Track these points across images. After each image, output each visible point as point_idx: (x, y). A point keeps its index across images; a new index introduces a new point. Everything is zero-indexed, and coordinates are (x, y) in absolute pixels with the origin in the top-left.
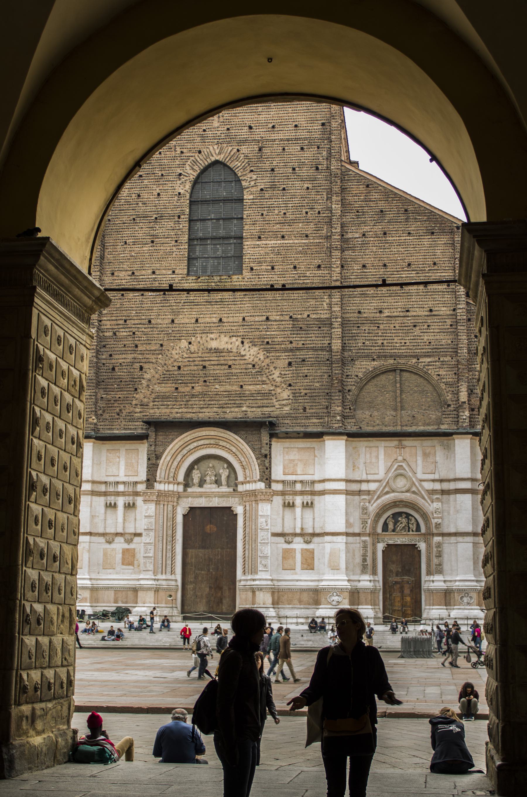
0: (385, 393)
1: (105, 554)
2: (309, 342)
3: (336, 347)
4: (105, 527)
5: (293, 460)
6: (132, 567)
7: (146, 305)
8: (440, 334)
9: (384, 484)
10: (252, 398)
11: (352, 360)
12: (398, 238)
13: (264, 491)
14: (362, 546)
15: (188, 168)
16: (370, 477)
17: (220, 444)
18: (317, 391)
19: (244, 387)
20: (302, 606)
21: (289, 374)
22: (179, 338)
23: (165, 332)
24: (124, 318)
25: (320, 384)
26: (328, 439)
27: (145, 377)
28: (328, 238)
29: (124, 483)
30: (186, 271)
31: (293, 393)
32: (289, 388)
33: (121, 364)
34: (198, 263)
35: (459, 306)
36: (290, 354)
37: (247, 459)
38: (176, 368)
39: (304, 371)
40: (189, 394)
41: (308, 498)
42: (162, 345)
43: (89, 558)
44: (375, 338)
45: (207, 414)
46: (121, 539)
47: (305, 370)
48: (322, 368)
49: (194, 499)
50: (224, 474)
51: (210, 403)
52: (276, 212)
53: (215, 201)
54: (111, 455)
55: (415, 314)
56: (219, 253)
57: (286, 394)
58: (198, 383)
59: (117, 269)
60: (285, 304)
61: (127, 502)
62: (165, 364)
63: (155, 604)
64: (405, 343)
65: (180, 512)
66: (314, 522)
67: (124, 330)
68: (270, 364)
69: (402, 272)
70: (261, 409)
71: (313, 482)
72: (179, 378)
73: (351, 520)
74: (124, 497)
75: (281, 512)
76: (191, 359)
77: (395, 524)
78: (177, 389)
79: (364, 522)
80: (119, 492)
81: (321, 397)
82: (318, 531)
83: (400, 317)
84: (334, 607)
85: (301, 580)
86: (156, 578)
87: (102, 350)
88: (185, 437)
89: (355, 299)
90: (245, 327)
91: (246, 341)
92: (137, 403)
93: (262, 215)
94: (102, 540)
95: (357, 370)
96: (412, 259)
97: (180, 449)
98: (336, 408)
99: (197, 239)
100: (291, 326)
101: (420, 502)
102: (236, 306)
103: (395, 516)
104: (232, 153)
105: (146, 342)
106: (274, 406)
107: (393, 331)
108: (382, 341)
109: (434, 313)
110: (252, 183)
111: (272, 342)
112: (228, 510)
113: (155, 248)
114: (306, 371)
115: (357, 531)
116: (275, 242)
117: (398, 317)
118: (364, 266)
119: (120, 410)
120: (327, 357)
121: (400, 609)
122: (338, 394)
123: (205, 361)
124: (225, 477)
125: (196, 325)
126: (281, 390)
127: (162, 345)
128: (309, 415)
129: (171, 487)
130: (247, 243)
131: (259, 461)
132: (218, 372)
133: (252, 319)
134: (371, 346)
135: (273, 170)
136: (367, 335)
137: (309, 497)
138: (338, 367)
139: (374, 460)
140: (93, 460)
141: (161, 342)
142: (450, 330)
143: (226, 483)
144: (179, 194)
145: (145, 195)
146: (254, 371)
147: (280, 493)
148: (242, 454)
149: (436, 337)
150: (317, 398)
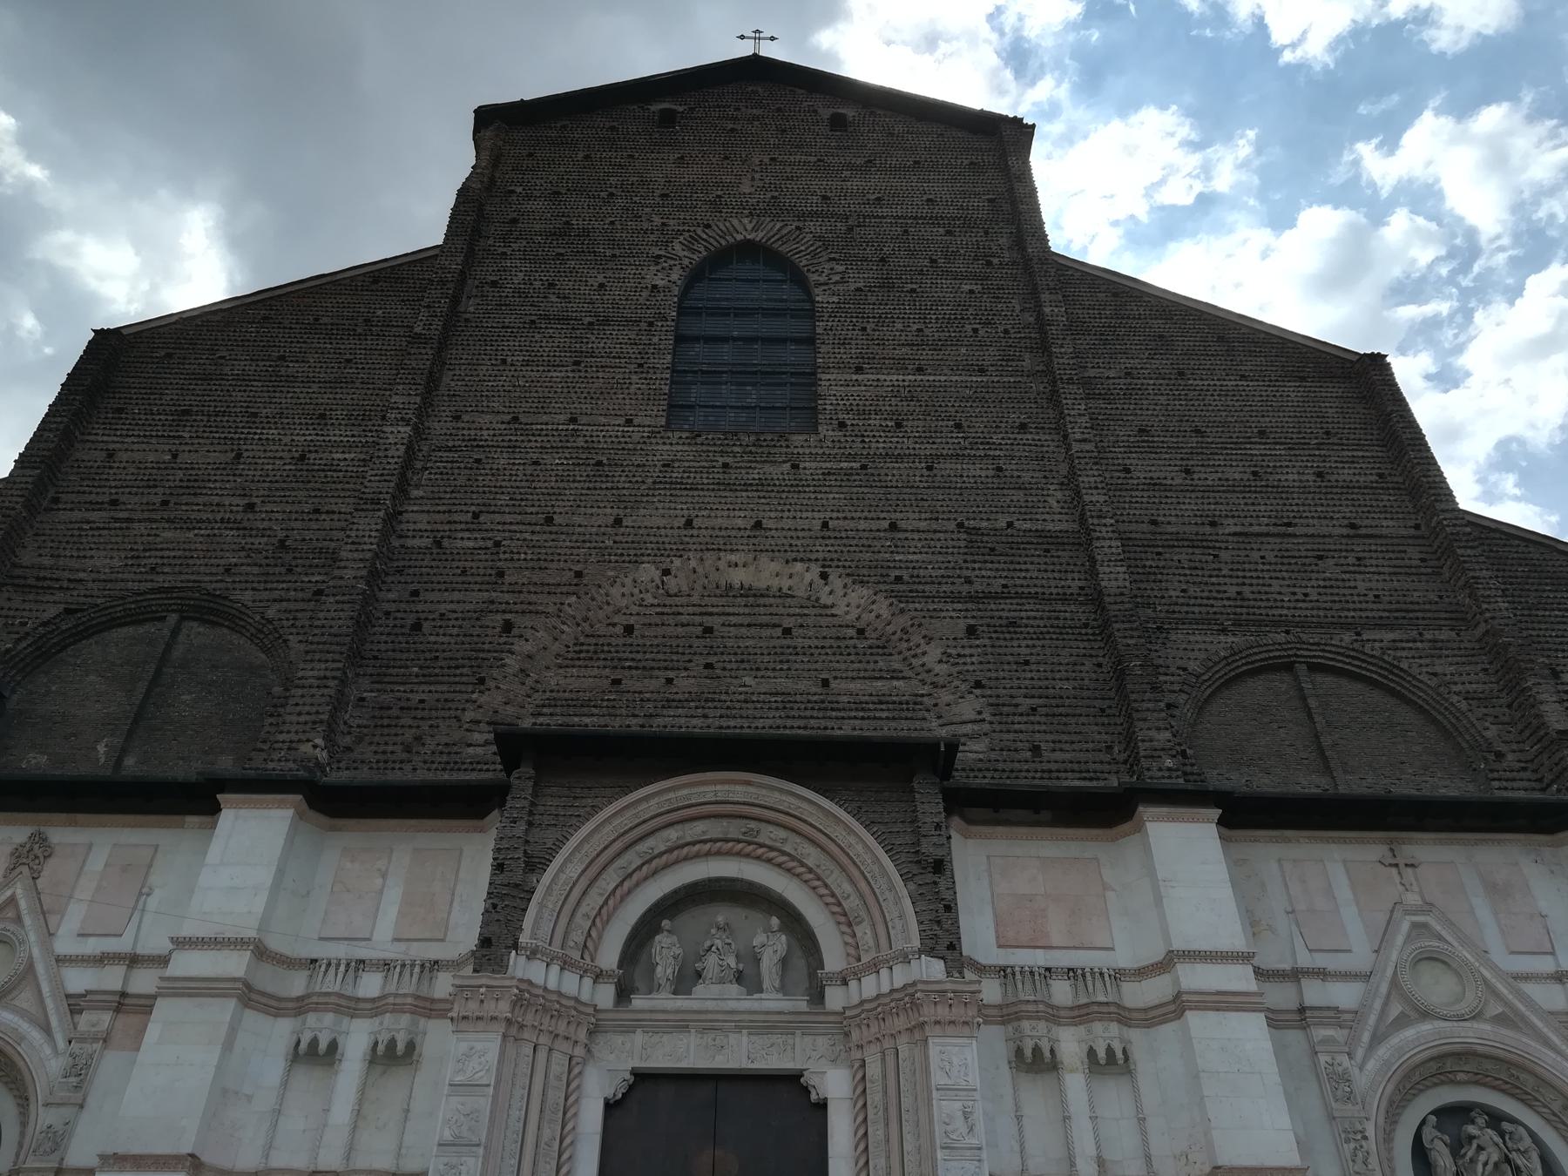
0: (1275, 726)
3: (1114, 583)
4: (269, 1147)
7: (540, 484)
8: (1400, 578)
9: (1384, 988)
10: (861, 714)
11: (1158, 628)
13: (949, 986)
15: (678, 247)
16: (1321, 961)
17: (760, 840)
18: (1067, 702)
19: (833, 684)
21: (971, 655)
23: (594, 544)
24: (473, 508)
26: (1158, 819)
27: (516, 648)
29: (386, 966)
30: (663, 421)
31: (992, 705)
32: (978, 692)
36: (969, 606)
37: (863, 885)
38: (619, 630)
39: (1016, 650)
40: (655, 696)
41: (1106, 1034)
42: (579, 574)
44: (1214, 580)
48: (1073, 644)
49: (656, 1038)
50: (773, 946)
55: (1311, 531)
57: (968, 708)
58: (686, 669)
60: (941, 497)
61: (384, 1038)
64: (1306, 595)
65: (597, 1089)
66: (1144, 1133)
67: (466, 535)
68: (910, 630)
71: (1118, 975)
74: (377, 1020)
78: (617, 682)
80: (358, 1000)
81: (1083, 720)
83: (1273, 535)
89: (1134, 494)
93: (864, 329)
97: (618, 845)
98: (1153, 733)
100: (962, 544)
101: (1547, 1060)
102: (802, 495)
105: (531, 564)
109: (1363, 531)
111: (912, 576)
112: (792, 1081)
113: (582, 374)
114: (1024, 651)
116: (901, 377)
117: (1267, 535)
119: (418, 739)
123: (711, 614)
124: (776, 959)
126: (952, 697)
128: (1053, 766)
129: (570, 983)
131: (912, 886)
132: (750, 642)
134: (1208, 598)
136: (1188, 572)
138: (1132, 629)
140: (280, 873)
141: (578, 568)
142: (1423, 570)
143: (777, 984)
144: (655, 287)
146: (861, 644)
147: (994, 1012)
148: (843, 869)
150: (1073, 720)
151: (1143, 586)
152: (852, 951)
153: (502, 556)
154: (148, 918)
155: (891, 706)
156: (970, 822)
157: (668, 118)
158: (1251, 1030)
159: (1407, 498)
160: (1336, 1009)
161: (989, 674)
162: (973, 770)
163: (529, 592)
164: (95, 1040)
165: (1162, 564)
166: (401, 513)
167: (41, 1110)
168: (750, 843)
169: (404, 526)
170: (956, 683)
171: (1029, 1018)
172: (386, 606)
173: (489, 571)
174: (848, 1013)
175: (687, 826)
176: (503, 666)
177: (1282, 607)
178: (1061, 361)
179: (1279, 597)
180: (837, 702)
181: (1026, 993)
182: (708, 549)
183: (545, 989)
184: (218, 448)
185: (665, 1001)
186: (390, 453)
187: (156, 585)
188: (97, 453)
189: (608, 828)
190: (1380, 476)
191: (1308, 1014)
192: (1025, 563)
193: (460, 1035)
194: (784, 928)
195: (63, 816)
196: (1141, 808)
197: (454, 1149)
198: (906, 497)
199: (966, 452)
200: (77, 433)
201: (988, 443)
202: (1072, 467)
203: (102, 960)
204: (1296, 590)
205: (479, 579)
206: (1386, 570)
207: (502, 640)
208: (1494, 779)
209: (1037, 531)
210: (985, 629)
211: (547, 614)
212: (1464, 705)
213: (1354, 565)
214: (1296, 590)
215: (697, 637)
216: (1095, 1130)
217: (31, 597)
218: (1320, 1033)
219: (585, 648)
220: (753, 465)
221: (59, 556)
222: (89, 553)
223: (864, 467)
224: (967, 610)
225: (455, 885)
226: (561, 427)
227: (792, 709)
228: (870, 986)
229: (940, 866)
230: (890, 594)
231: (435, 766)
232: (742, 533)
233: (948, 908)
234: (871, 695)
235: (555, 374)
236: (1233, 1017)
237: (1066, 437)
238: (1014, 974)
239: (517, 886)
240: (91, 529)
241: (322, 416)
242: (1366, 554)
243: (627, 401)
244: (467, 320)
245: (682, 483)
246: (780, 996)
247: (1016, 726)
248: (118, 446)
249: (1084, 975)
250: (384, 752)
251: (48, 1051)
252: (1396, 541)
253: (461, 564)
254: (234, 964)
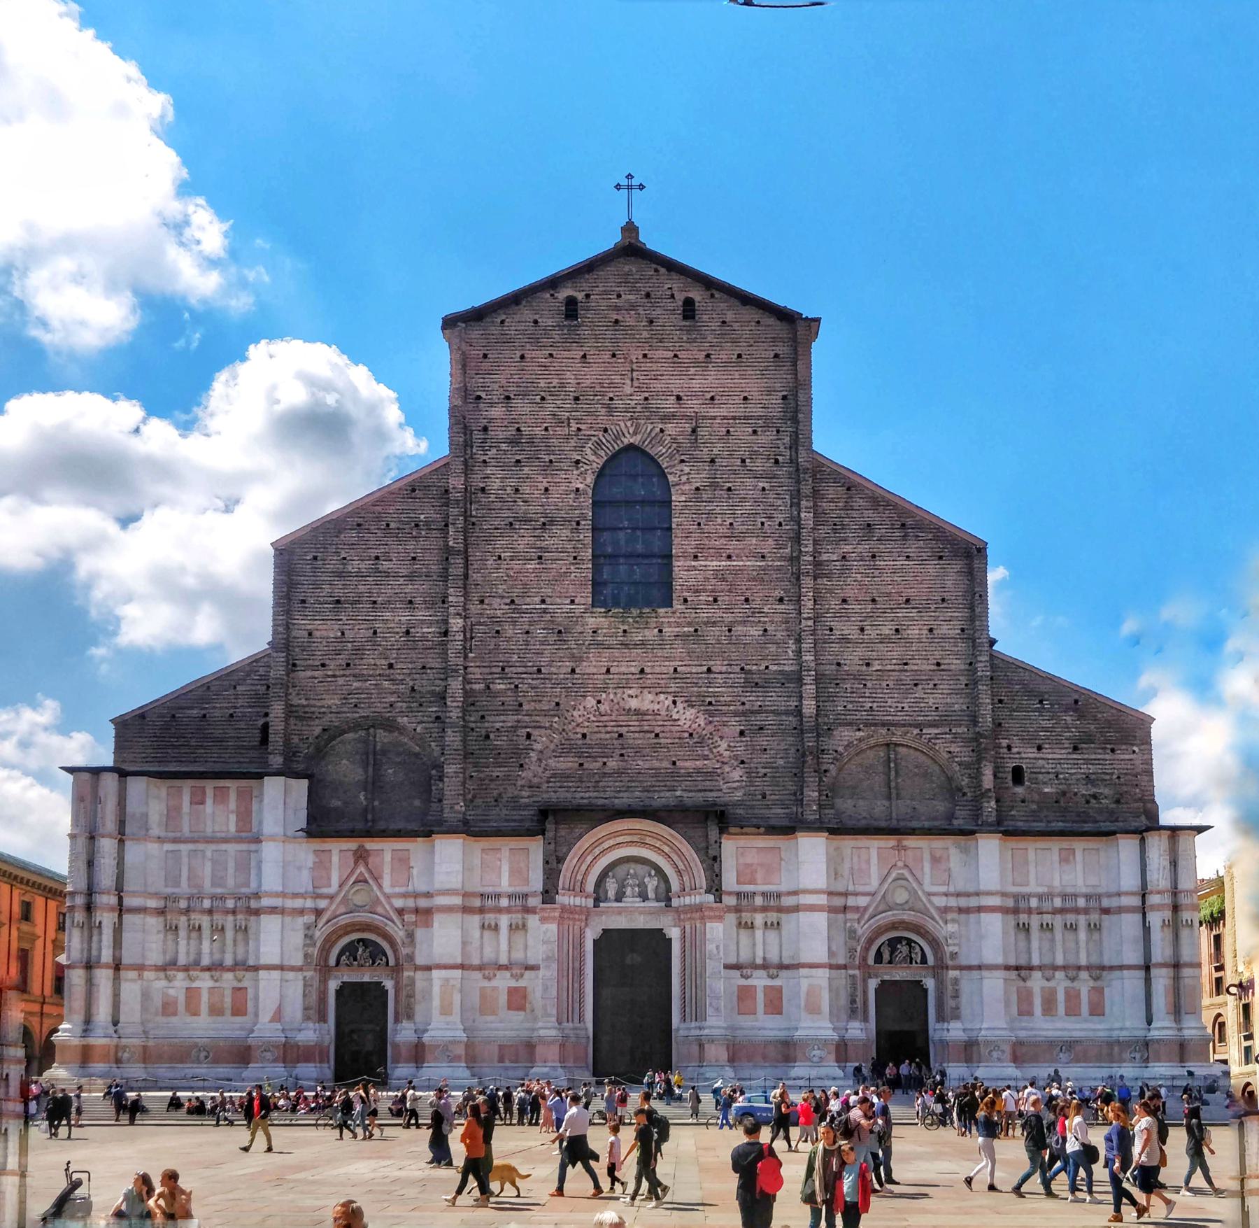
1: (483, 996)
5: (752, 865)
6: (522, 1013)
11: (829, 729)
12: (892, 563)
15: (589, 451)
16: (860, 889)
19: (678, 763)
20: (767, 1064)
27: (534, 747)
28: (794, 560)
34: (607, 591)
35: (980, 658)
36: (743, 718)
38: (579, 736)
41: (773, 917)
42: (558, 704)
45: (624, 800)
46: (507, 974)
47: (763, 741)
50: (652, 884)
51: (629, 784)
52: (719, 521)
53: (629, 503)
55: (915, 668)
56: (637, 577)
57: (737, 774)
62: (564, 730)
70: (702, 794)
71: (779, 895)
73: (834, 948)
76: (600, 724)
78: (581, 765)
79: (852, 951)
82: (786, 961)
85: (765, 1029)
87: (469, 709)
91: (679, 700)
93: (699, 524)
94: (477, 975)
96: (911, 593)
98: (811, 793)
99: (605, 557)
100: (742, 681)
101: (930, 925)
103: (893, 943)
104: (653, 434)
106: (721, 790)
108: (870, 705)
109: (942, 667)
110: (684, 478)
114: (766, 743)
115: (841, 961)
116: (718, 563)
118: (844, 601)
119: (500, 795)
122: (813, 774)
125: (606, 676)
127: (558, 704)
129: (578, 901)
130: (678, 564)
132: (640, 742)
133: (688, 669)
135: (713, 461)
137: (775, 914)
139: (864, 866)
141: (557, 700)
144: (578, 490)
145: (525, 489)
148: (679, 856)
157: (571, 303)
158: (821, 919)
178: (805, 558)
186: (457, 638)
190: (963, 630)
204: (899, 705)
211: (546, 728)
212: (957, 768)
216: (764, 950)
222: (324, 696)
223: (696, 631)
228: (687, 900)
229: (715, 859)
232: (634, 677)
235: (529, 566)
236: (816, 914)
237: (800, 613)
241: (411, 602)
244: (474, 524)
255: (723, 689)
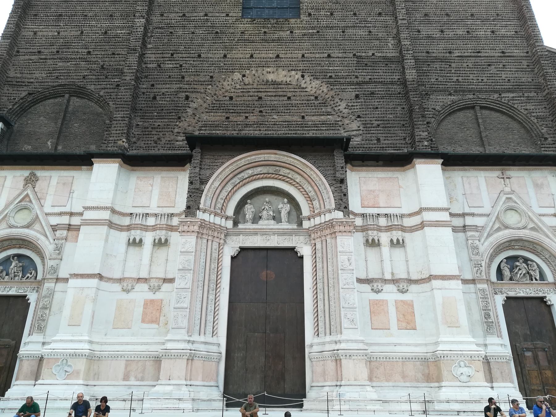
0: (466, 129)
2: (378, 77)
3: (411, 77)
6: (155, 326)
7: (195, 42)
8: (518, 73)
9: (494, 219)
10: (316, 128)
11: (426, 94)
13: (344, 220)
14: (480, 296)
16: (473, 210)
17: (280, 173)
18: (391, 122)
20: (408, 384)
21: (357, 106)
22: (231, 71)
23: (217, 65)
24: (171, 52)
25: (394, 115)
27: (191, 105)
29: (156, 215)
30: (240, 15)
31: (363, 124)
32: (358, 119)
33: (163, 93)
36: (357, 87)
37: (316, 188)
38: (227, 98)
39: (373, 103)
41: (397, 235)
42: (212, 77)
43: (94, 312)
44: (448, 75)
46: (144, 287)
48: (395, 100)
49: (247, 237)
50: (285, 208)
54: (142, 182)
55: (487, 55)
57: (355, 125)
58: (252, 113)
59: (167, 11)
60: (347, 44)
61: (157, 238)
62: (215, 94)
63: (186, 380)
64: (482, 80)
66: (407, 265)
67: (169, 62)
68: (335, 96)
69: (466, 21)
71: (402, 216)
72: (231, 108)
74: (154, 232)
75: (363, 252)
77: (511, 270)
78: (227, 118)
80: (147, 226)
81: (396, 129)
82: (414, 277)
84: (464, 384)
85: (400, 344)
86: (191, 339)
88: (238, 160)
89: (421, 41)
90: (304, 63)
92: (180, 131)
94: (117, 287)
95: (434, 103)
97: (231, 176)
98: (421, 133)
100: (355, 62)
101: (546, 241)
102: (295, 44)
103: (512, 260)
105: (194, 73)
107: (466, 69)
108: (456, 78)
109: (507, 54)
111: (336, 76)
112: (292, 250)
114: (376, 103)
115: (469, 276)
119: (159, 139)
120: (399, 90)
121: (540, 388)
123: (261, 92)
124: (286, 212)
126: (349, 121)
128: (384, 146)
129: (218, 220)
131: (333, 188)
132: (276, 103)
134: (446, 82)
136: (439, 72)
138: (416, 94)
140: (117, 185)
141: (211, 74)
142: (527, 70)
146: (316, 102)
147: (360, 228)
148: (309, 183)
149: (514, 76)
150: (392, 129)
151: (422, 78)
152: (312, 209)
153: (183, 70)
154: (74, 200)
155: (327, 125)
156: (353, 166)
159: (525, 41)
160: (476, 226)
161: (363, 113)
162: (355, 148)
163: (194, 84)
164: (62, 239)
165: (429, 69)
166: (144, 54)
167: (49, 261)
168: (277, 174)
169: (146, 59)
170: (351, 116)
171: (371, 230)
172: (143, 90)
173: (179, 77)
174: (310, 229)
175: (255, 169)
176: (187, 112)
177: (473, 85)
179: (472, 81)
180: (307, 124)
181: (370, 222)
182: (259, 67)
183: (210, 222)
184: (74, 29)
185: (249, 226)
187: (59, 84)
188: (30, 33)
189: (227, 170)
190: (516, 32)
191: (467, 227)
192: (378, 70)
193: (182, 237)
194: (289, 202)
195: (40, 167)
196: (414, 160)
197: (183, 271)
198: (334, 44)
199: (357, 25)
200: (22, 25)
201: (366, 21)
202: (398, 30)
203: (61, 214)
204: (479, 78)
205: (175, 80)
206: (514, 70)
207: (186, 103)
208: (542, 148)
209: (383, 57)
210: (362, 95)
212: (535, 121)
213: (502, 68)
214: (479, 78)
215: (256, 101)
216: (392, 266)
217: (15, 89)
218: (469, 234)
219: (215, 105)
220: (275, 32)
221: (23, 73)
223: (318, 32)
224: (356, 88)
225: (176, 189)
226: (201, 18)
227: (291, 127)
228: (318, 220)
229: (342, 181)
230: (328, 83)
231: (166, 148)
232: (272, 60)
233: (345, 195)
234: (320, 121)
237: (396, 18)
238: (366, 216)
239: (197, 189)
240: (33, 62)
241: (111, 16)
242: (507, 64)
243: (226, 7)
245: (248, 40)
246: (288, 224)
247: (372, 132)
248: (37, 30)
249: (390, 216)
250: (148, 144)
251: (47, 243)
252: (519, 58)
253: (168, 74)
254: (106, 215)
255: (341, 68)
